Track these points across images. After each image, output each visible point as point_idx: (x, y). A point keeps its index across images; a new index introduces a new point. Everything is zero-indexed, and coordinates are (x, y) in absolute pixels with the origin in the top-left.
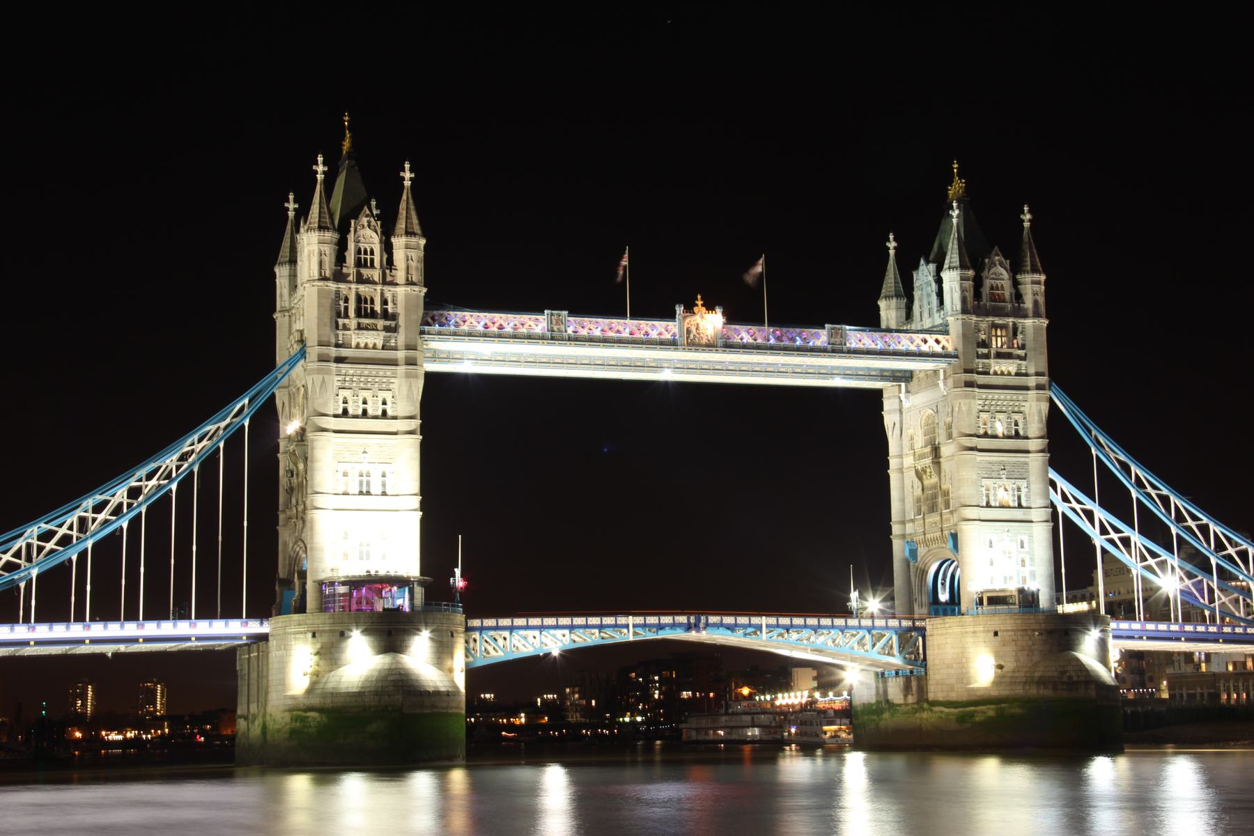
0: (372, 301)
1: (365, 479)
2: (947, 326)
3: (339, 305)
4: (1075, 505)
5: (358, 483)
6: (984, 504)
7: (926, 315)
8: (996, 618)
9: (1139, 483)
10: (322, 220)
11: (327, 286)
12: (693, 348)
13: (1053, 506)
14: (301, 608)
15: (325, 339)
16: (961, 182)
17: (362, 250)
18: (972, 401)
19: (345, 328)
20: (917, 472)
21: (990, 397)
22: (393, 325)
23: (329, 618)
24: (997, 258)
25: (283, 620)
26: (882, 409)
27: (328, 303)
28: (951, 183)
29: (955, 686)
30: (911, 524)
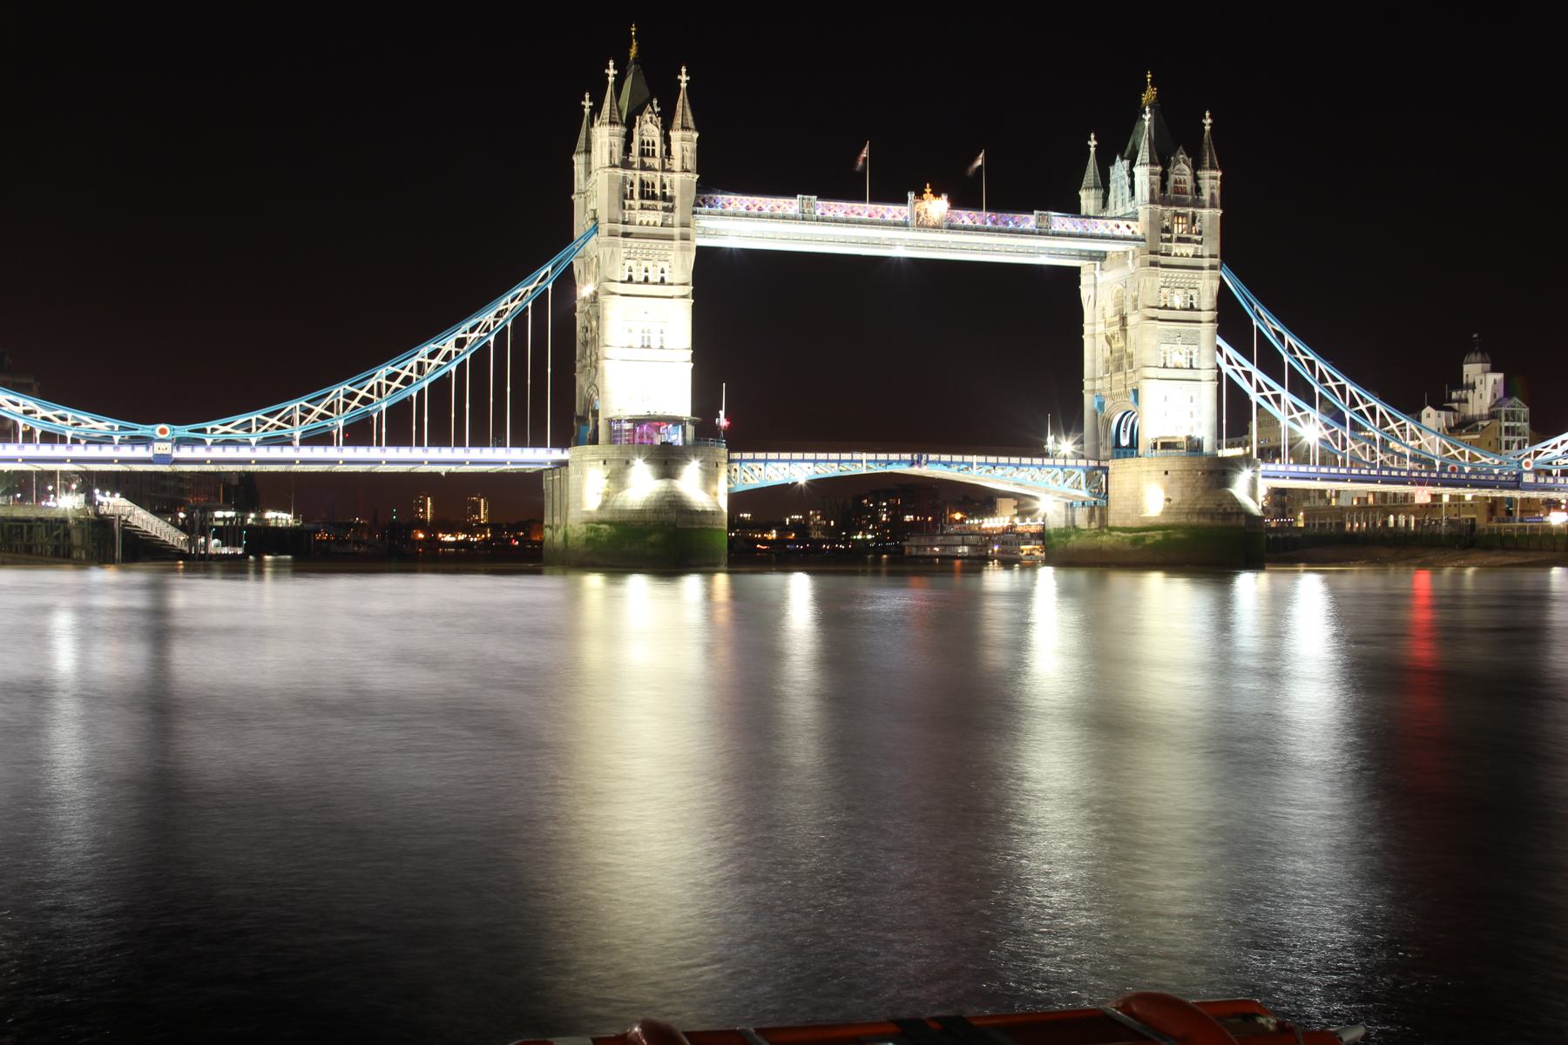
0: (653, 186)
2: (1137, 214)
4: (1236, 366)
5: (641, 339)
6: (1162, 366)
7: (1119, 204)
9: (1291, 350)
12: (922, 229)
13: (1219, 368)
15: (614, 217)
18: (1156, 278)
19: (631, 208)
20: (1107, 337)
21: (1171, 275)
24: (1181, 156)
26: (1079, 282)
27: (616, 187)
30: (1100, 381)
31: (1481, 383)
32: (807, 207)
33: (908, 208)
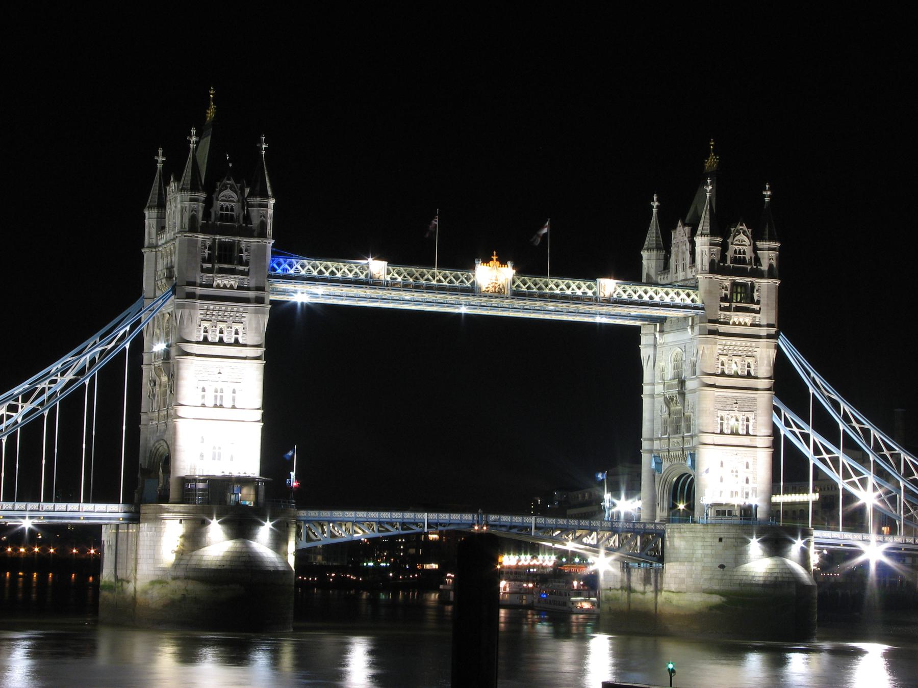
1: (219, 394)
3: (204, 252)
4: (795, 429)
6: (719, 432)
7: (680, 269)
9: (846, 418)
13: (775, 431)
14: (164, 498)
18: (714, 346)
20: (665, 398)
24: (741, 227)
25: (153, 507)
28: (707, 157)
29: (686, 580)
30: (658, 442)
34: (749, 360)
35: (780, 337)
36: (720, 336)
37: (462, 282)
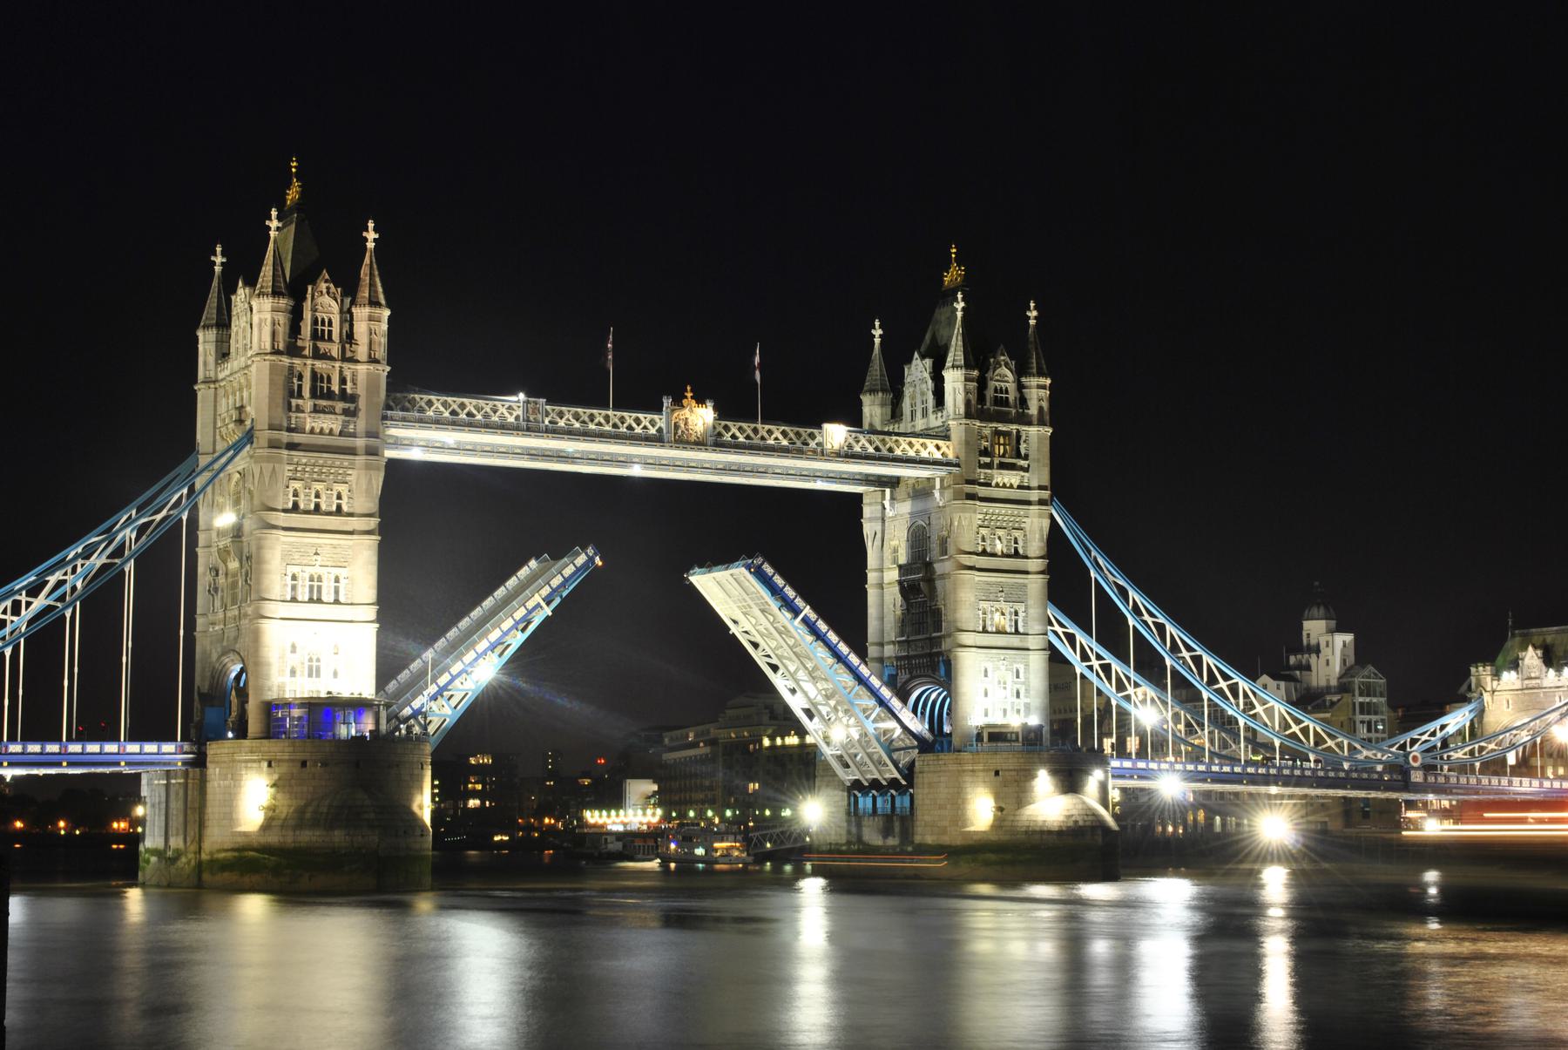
1: (316, 584)
2: (949, 430)
3: (293, 383)
6: (981, 629)
7: (919, 414)
8: (998, 756)
9: (1136, 610)
10: (277, 284)
11: (281, 361)
12: (681, 446)
14: (242, 733)
16: (960, 269)
17: (320, 320)
18: (973, 515)
19: (299, 409)
22: (352, 409)
23: (289, 746)
24: (1002, 358)
25: (230, 745)
26: (861, 516)
27: (280, 380)
29: (948, 829)
31: (1327, 646)
32: (534, 413)
33: (664, 417)
34: (1017, 534)
35: (1054, 503)
36: (981, 501)
37: (645, 428)
